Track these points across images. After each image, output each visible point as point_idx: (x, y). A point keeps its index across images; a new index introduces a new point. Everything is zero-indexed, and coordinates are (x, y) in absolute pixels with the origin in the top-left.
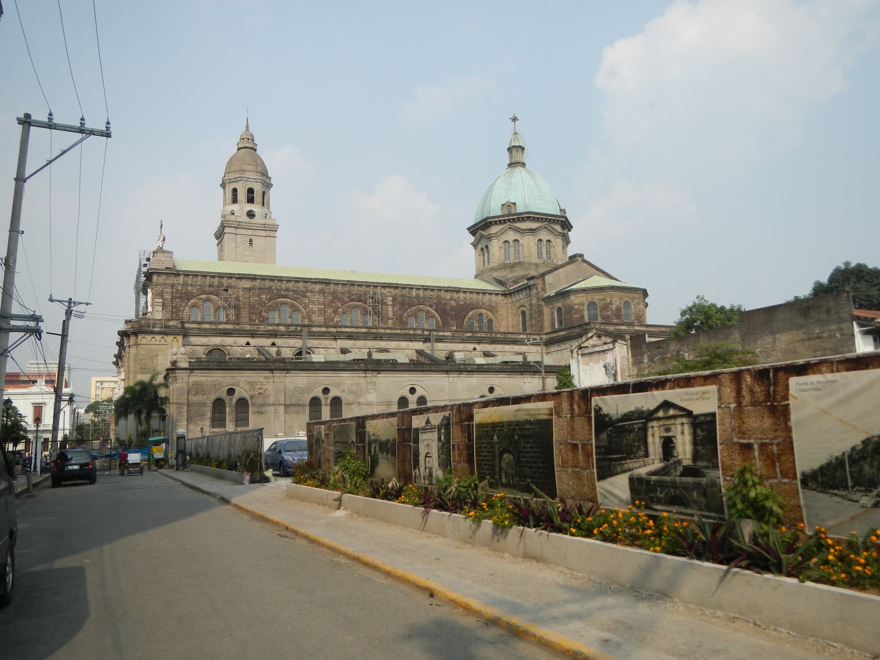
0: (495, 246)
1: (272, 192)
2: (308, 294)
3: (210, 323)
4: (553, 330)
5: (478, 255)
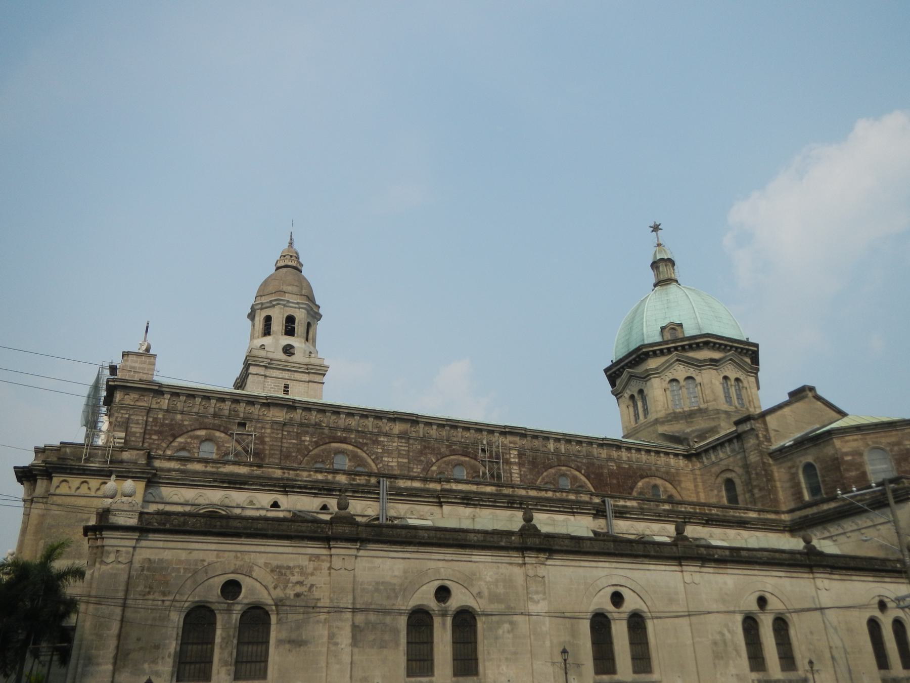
0: (657, 389)
1: (321, 328)
2: (382, 439)
3: (206, 461)
4: (800, 505)
5: (624, 406)
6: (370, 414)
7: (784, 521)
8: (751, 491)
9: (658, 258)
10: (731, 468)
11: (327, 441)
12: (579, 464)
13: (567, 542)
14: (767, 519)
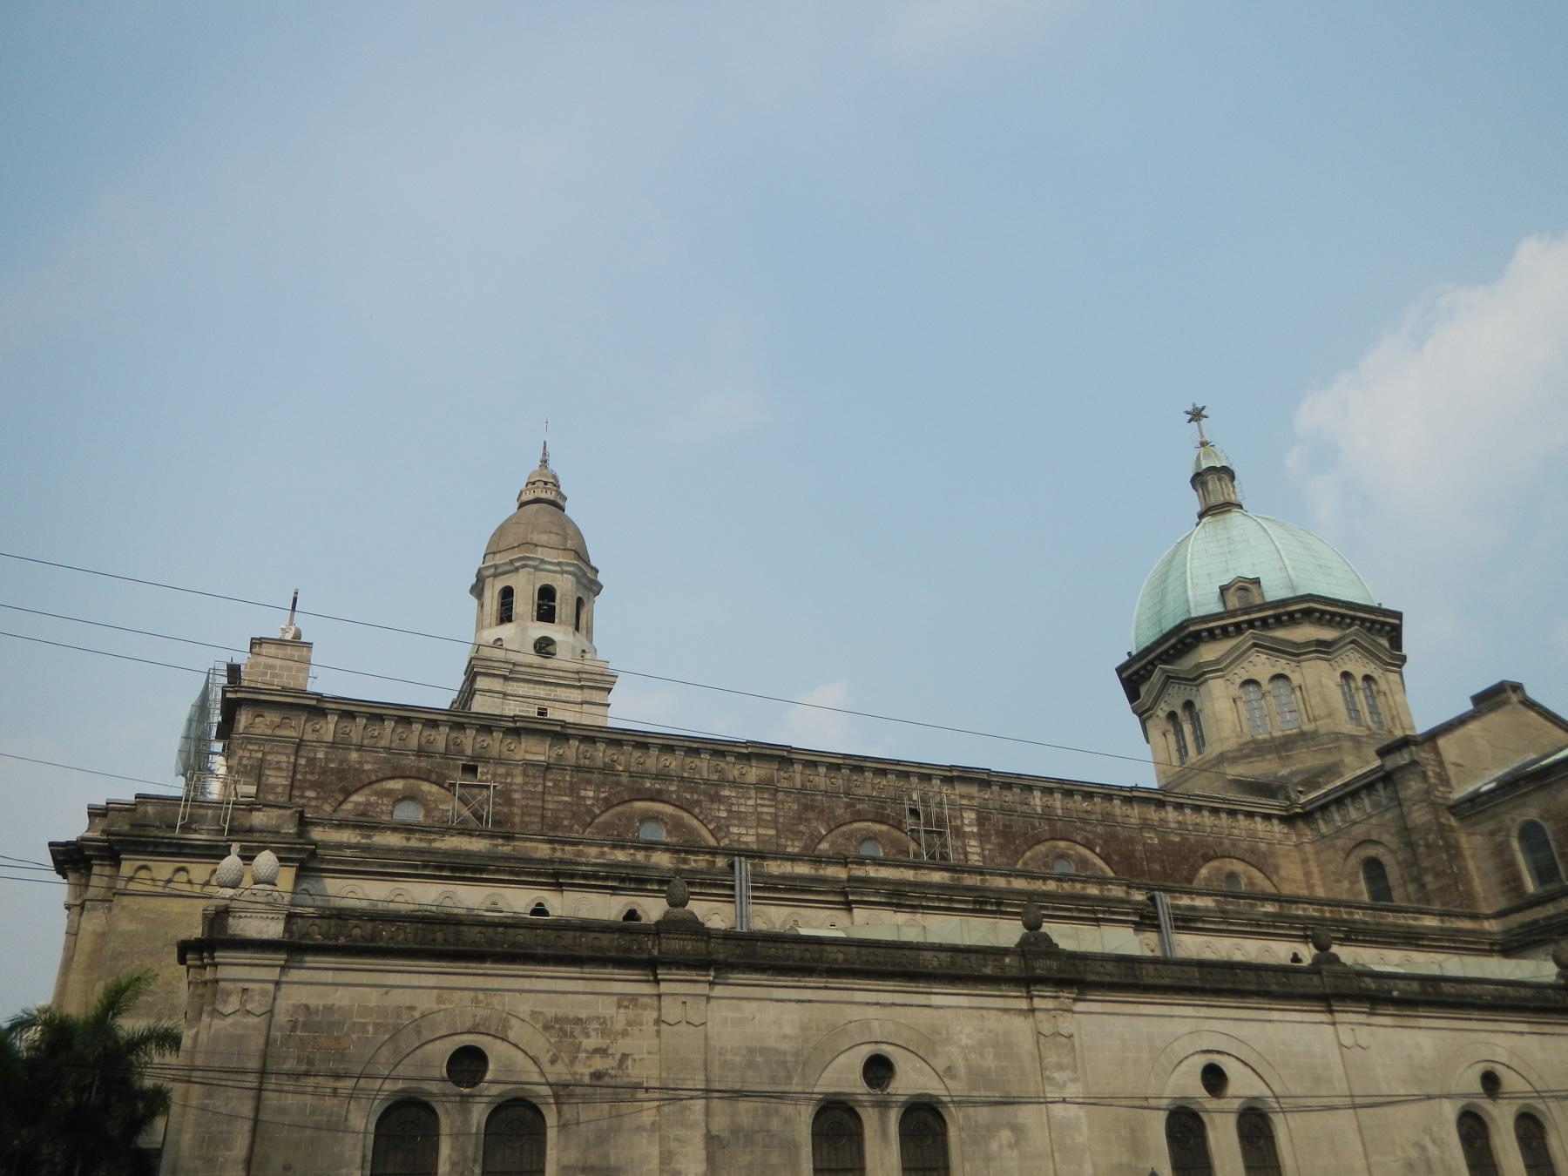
1: (600, 607)
2: (727, 793)
3: (407, 829)
4: (1518, 902)
6: (704, 746)
7: (1490, 933)
8: (1418, 880)
9: (1204, 467)
10: (1374, 837)
11: (627, 798)
12: (1091, 836)
13: (1110, 967)
14: (1459, 930)
